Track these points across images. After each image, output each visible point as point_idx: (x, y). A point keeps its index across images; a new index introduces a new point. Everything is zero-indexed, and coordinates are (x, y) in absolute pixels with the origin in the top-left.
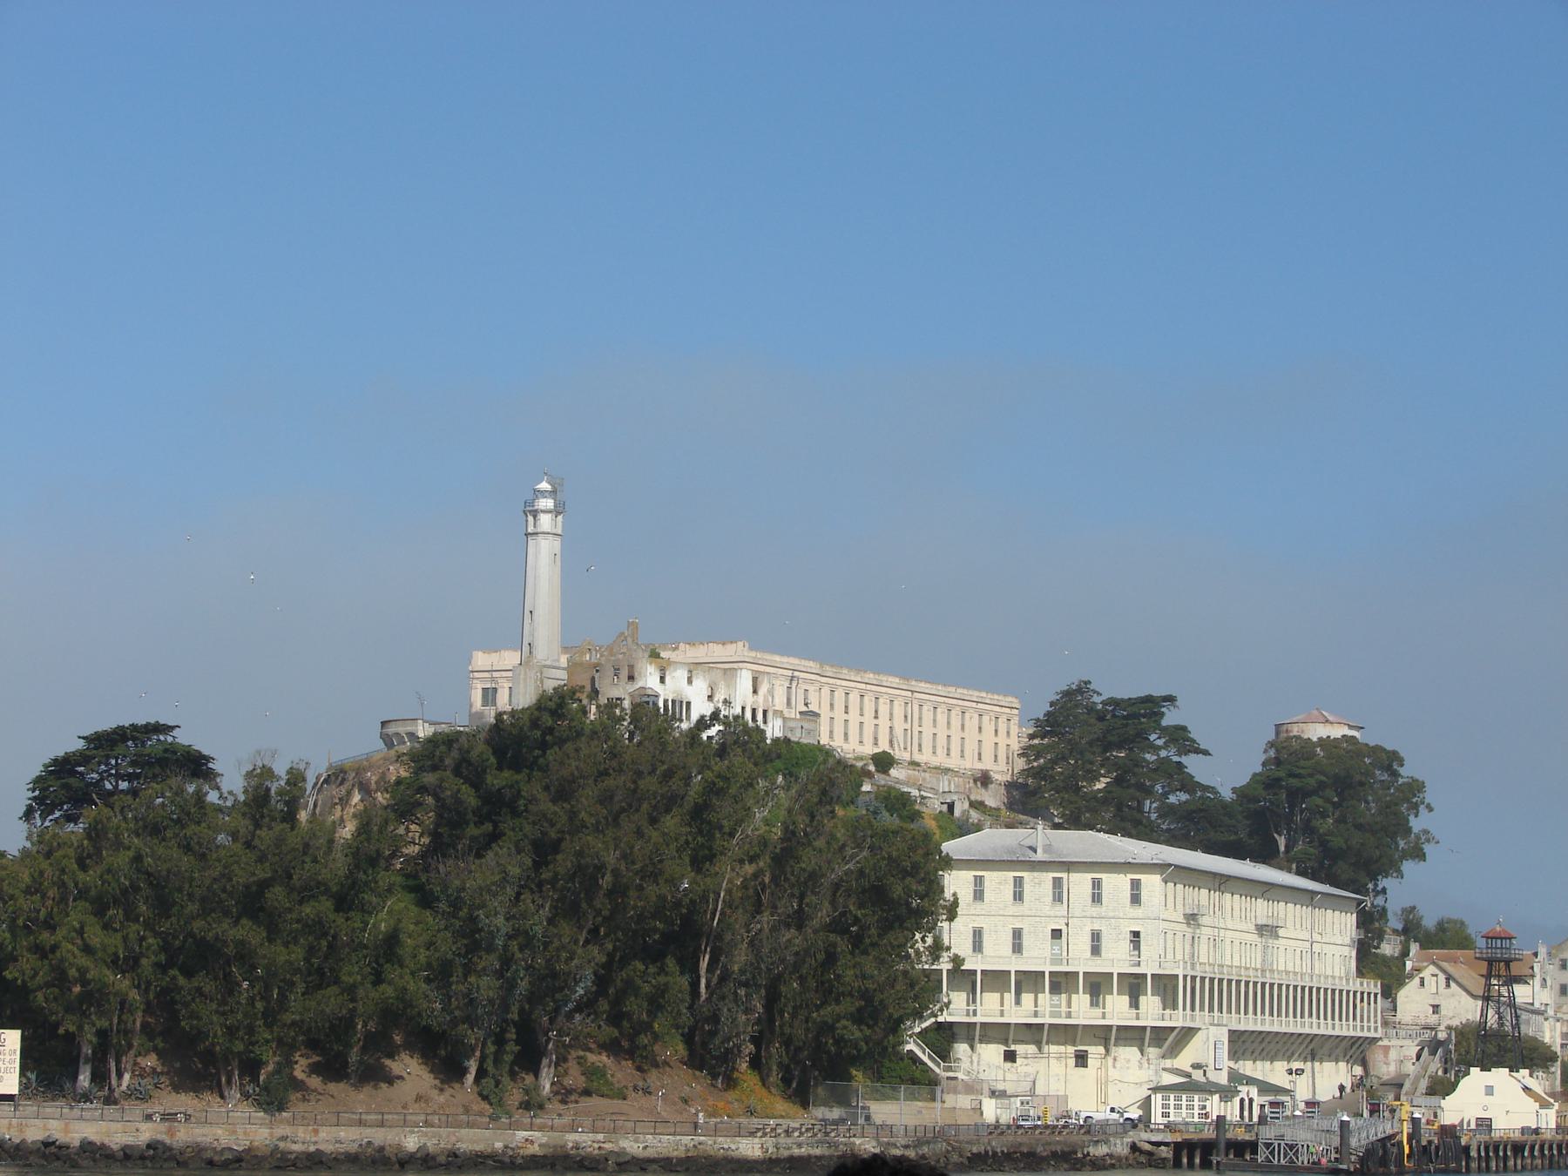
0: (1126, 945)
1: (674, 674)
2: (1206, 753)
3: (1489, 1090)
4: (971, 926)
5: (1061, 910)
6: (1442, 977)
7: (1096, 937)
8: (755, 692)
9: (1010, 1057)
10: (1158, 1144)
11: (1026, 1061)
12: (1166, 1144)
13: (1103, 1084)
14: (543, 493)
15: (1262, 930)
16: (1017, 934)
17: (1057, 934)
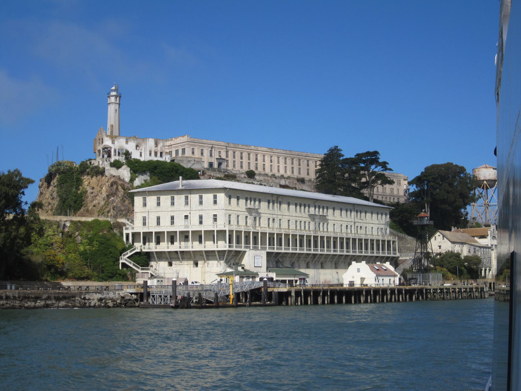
0: (211, 220)
1: (119, 140)
2: (390, 170)
3: (359, 270)
4: (156, 216)
5: (188, 208)
6: (441, 236)
7: (201, 217)
8: (156, 145)
9: (170, 264)
10: (131, 294)
11: (176, 266)
12: (135, 294)
13: (204, 273)
14: (112, 91)
15: (313, 217)
16: (172, 218)
17: (186, 217)
